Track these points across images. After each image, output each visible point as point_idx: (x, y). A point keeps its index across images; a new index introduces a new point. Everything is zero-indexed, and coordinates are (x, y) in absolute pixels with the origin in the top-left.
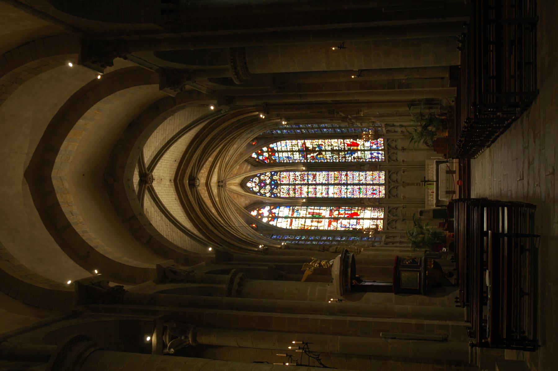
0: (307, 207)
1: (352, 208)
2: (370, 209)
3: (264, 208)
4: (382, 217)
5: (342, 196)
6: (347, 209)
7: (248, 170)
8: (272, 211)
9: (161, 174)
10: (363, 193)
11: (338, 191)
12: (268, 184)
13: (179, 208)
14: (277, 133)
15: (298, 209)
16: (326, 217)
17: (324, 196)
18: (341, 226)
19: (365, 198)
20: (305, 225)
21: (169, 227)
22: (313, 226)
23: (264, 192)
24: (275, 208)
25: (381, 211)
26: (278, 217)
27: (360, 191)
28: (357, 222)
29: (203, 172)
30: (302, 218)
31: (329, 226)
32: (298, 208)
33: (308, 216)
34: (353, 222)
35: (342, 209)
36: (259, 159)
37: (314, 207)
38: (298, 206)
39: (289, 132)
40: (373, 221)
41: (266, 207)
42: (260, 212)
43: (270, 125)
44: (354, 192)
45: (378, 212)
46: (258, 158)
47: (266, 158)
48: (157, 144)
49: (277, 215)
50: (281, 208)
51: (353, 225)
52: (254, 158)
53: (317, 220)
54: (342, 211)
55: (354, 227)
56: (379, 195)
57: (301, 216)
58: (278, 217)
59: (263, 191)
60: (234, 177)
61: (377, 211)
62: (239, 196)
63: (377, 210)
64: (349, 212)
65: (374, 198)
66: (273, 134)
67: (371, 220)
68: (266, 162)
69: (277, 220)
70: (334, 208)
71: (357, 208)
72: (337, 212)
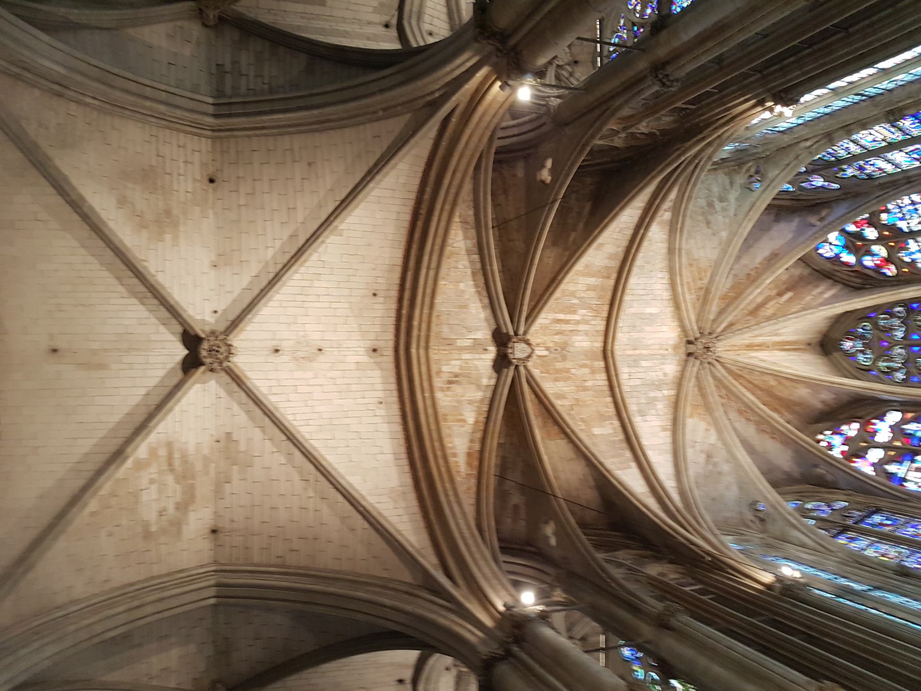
3: (881, 418)
7: (820, 301)
9: (317, 336)
12: (897, 343)
13: (385, 427)
14: (880, 169)
21: (312, 481)
23: (888, 368)
29: (577, 317)
36: (866, 267)
39: (916, 156)
43: (808, 143)
46: (859, 262)
47: (888, 261)
48: (270, 252)
52: (846, 264)
59: (885, 364)
60: (753, 328)
62: (783, 381)
66: (870, 177)
68: (884, 274)
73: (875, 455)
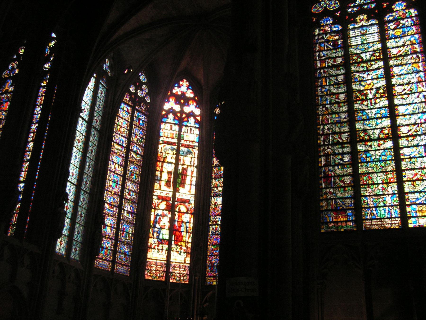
0: (196, 167)
1: (191, 233)
2: (187, 262)
4: (171, 281)
5: (211, 218)
6: (188, 224)
8: (192, 118)
10: (214, 250)
11: (218, 211)
15: (193, 154)
16: (177, 193)
17: (213, 191)
18: (157, 215)
19: (207, 253)
20: (164, 162)
22: (161, 174)
24: (196, 121)
25: (182, 278)
26: (181, 126)
27: (217, 245)
28: (164, 240)
30: (178, 159)
31: (159, 197)
32: (195, 153)
33: (180, 167)
34: (165, 234)
35: (190, 218)
37: (196, 177)
38: (198, 153)
40: (164, 266)
41: (199, 110)
42: (191, 102)
44: (217, 236)
45: (182, 274)
49: (185, 123)
50: (197, 129)
51: (157, 233)
53: (172, 181)
54: (186, 218)
55: (155, 235)
56: (210, 277)
57: (181, 157)
58: (181, 126)
61: (182, 272)
63: (185, 272)
64: (183, 229)
65: (206, 268)
67: (166, 262)
69: (175, 124)
70: (193, 205)
71: (190, 240)
72: (183, 209)
73: (177, 108)
